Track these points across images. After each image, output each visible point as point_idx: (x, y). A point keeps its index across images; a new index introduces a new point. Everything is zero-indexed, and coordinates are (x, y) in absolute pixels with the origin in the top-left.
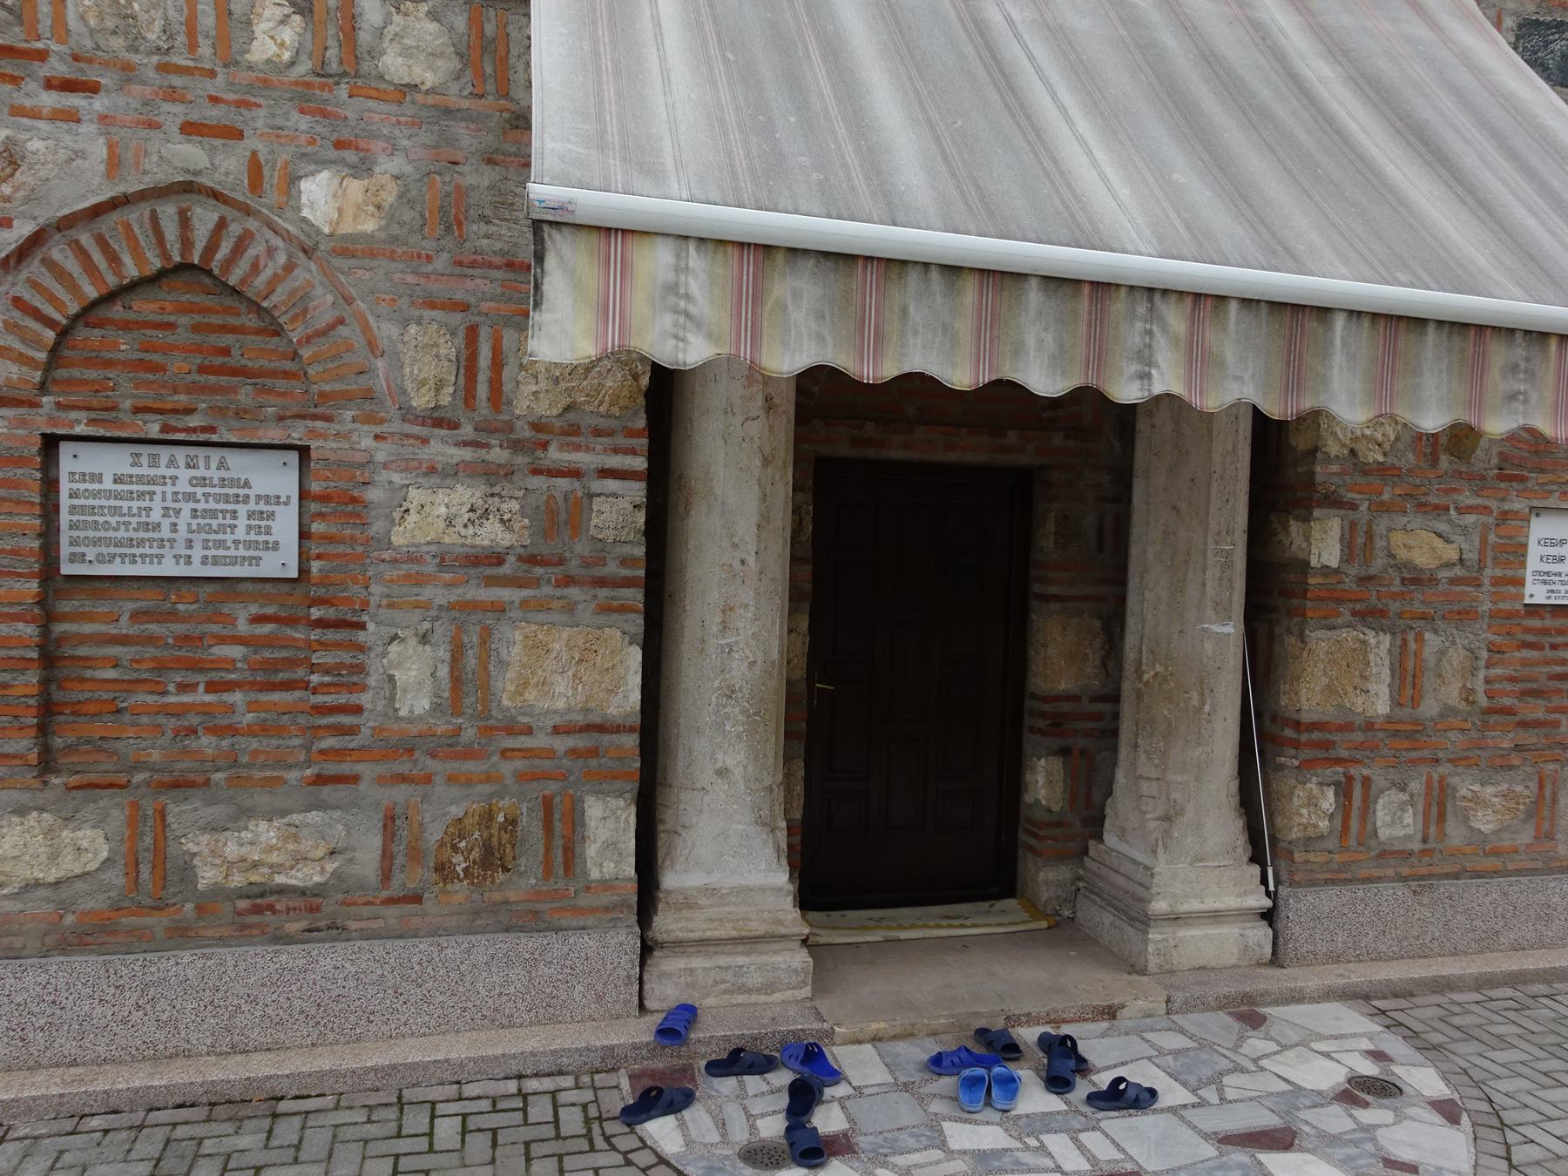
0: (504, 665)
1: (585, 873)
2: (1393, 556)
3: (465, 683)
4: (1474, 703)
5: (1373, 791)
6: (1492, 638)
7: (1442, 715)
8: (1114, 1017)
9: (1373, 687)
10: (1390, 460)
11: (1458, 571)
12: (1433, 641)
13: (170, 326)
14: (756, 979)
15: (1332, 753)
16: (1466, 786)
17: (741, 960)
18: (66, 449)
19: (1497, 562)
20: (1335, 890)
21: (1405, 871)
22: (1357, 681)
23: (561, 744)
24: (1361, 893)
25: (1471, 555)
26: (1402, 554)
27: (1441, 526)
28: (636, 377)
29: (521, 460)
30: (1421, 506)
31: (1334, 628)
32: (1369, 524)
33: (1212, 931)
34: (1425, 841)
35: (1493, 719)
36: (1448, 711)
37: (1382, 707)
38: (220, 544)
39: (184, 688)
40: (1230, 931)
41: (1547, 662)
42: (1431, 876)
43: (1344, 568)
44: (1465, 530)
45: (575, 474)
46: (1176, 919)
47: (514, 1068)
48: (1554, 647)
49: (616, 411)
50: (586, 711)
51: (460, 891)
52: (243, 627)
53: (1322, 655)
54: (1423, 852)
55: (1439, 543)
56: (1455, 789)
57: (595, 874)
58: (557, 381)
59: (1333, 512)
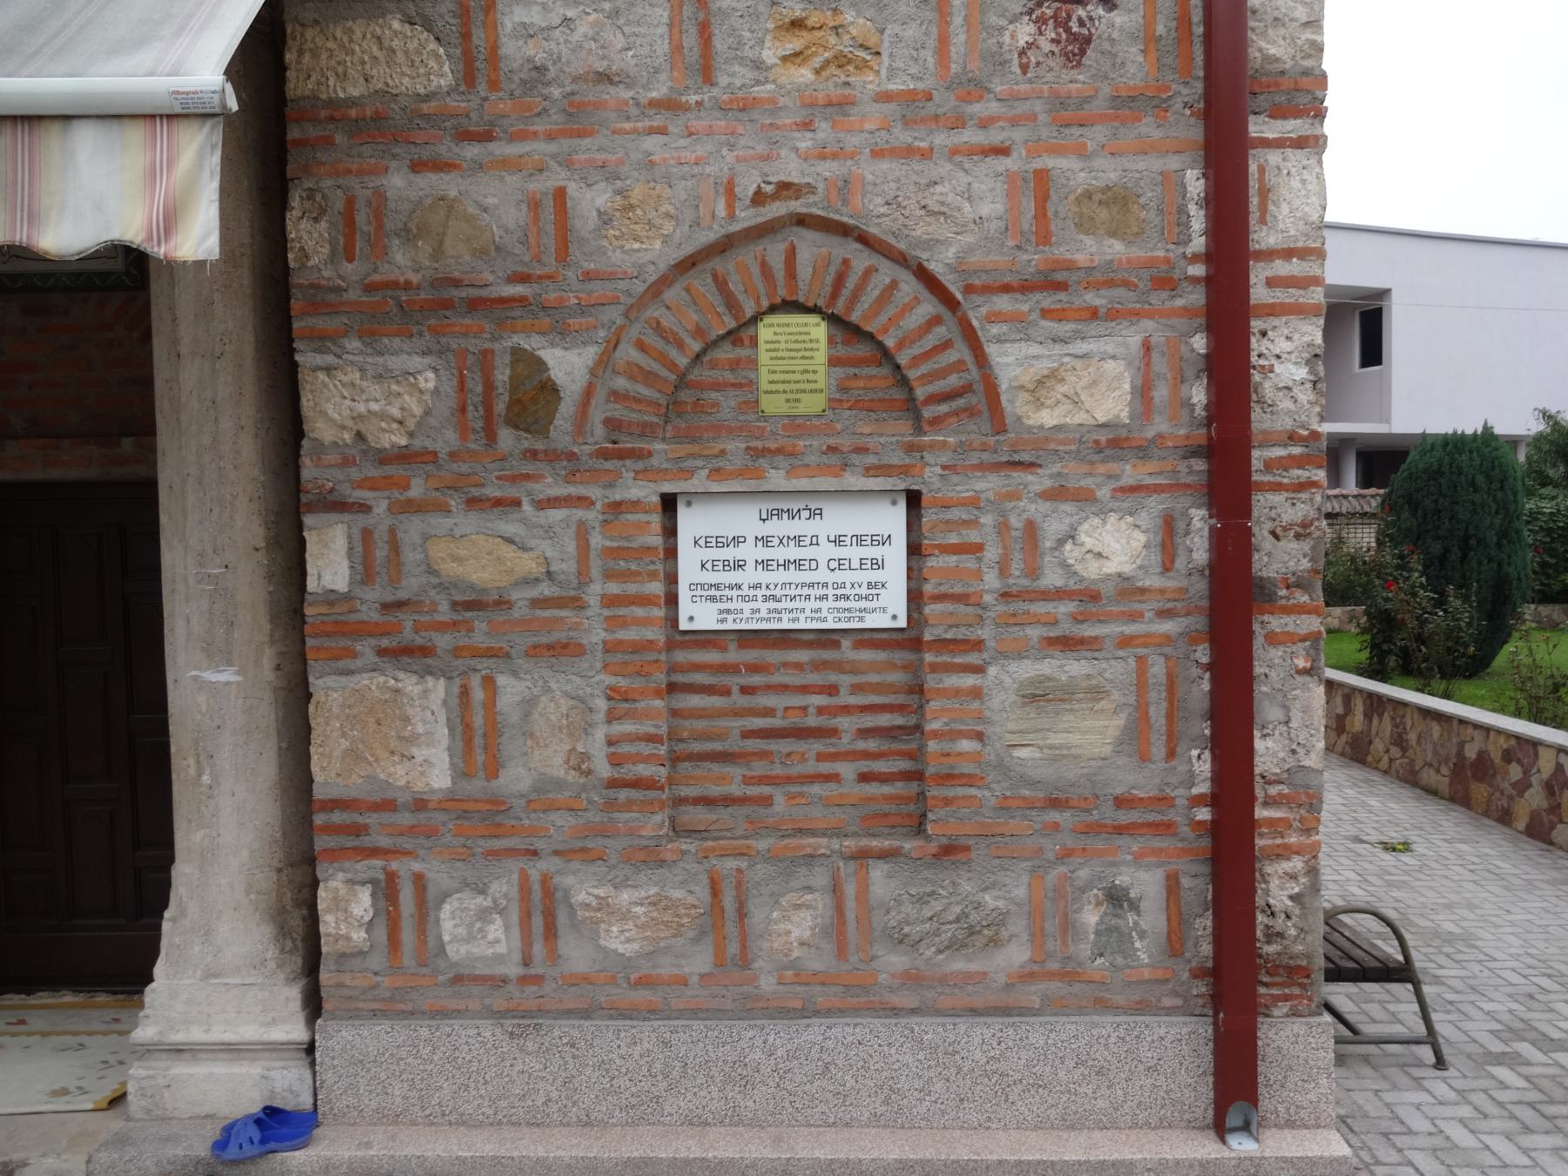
2: (436, 573)
4: (589, 772)
5: (431, 892)
6: (609, 680)
7: (536, 789)
9: (419, 753)
10: (418, 443)
11: (546, 590)
12: (511, 690)
15: (366, 841)
16: (583, 888)
19: (609, 575)
20: (385, 1025)
21: (499, 1003)
24: (424, 1032)
25: (564, 566)
26: (450, 569)
27: (511, 528)
30: (473, 503)
31: (350, 673)
32: (392, 531)
34: (527, 961)
35: (623, 795)
36: (545, 785)
37: (439, 778)
40: (249, 1070)
41: (738, 713)
42: (542, 1012)
43: (357, 591)
44: (549, 532)
46: (178, 1051)
48: (745, 690)
53: (335, 710)
54: (523, 980)
55: (509, 552)
56: (567, 893)
59: (333, 517)
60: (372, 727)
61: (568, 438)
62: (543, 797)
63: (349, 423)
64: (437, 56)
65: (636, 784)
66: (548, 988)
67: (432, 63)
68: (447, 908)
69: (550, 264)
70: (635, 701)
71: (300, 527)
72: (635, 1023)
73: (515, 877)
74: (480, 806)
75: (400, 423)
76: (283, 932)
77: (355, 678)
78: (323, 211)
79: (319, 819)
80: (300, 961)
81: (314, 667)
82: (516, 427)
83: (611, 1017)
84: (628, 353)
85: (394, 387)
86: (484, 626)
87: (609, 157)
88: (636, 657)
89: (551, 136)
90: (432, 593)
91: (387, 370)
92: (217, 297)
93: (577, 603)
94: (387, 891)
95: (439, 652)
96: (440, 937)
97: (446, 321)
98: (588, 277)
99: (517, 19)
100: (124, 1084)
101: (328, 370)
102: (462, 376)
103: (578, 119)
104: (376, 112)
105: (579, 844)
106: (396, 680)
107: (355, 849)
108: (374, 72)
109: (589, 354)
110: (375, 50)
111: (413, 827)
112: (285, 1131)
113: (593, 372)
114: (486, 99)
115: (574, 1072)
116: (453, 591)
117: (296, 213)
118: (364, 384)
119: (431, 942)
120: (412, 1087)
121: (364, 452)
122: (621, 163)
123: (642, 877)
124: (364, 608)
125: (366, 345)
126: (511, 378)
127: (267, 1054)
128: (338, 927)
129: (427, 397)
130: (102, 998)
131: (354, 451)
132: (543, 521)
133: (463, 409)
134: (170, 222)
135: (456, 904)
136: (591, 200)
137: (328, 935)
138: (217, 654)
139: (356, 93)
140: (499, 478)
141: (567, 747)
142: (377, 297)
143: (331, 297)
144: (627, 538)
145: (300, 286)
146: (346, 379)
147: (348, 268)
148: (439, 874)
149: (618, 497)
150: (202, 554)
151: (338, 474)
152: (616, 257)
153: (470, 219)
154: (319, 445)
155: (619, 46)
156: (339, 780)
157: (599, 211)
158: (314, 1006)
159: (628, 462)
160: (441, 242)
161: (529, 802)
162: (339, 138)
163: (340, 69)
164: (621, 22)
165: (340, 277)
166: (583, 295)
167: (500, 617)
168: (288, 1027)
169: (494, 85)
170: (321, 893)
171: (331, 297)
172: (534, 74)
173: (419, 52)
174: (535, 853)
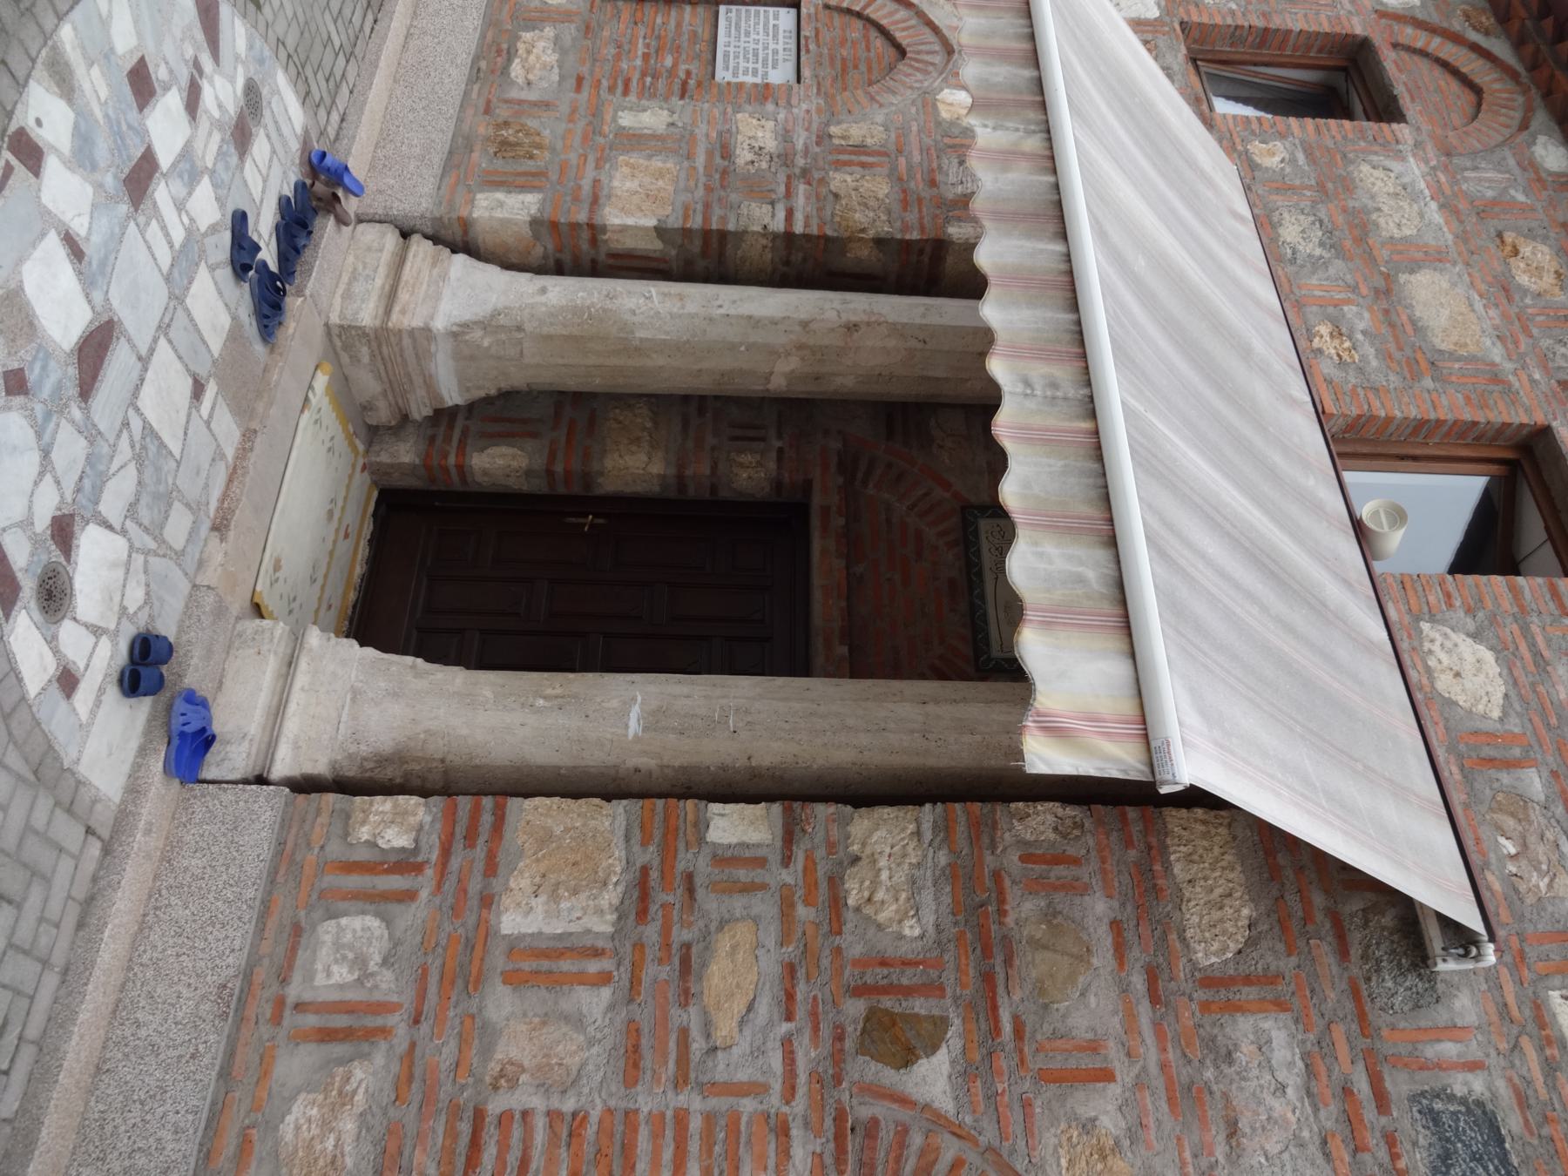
0: (650, 157)
1: (481, 191)
2: (720, 928)
3: (634, 141)
4: (496, 1088)
5: (394, 908)
6: (595, 1116)
8: (215, 528)
9: (539, 903)
10: (849, 916)
11: (698, 1045)
12: (594, 1002)
13: (868, 49)
14: (358, 288)
15: (458, 845)
16: (367, 1077)
17: (379, 282)
18: (793, 11)
19: (710, 1118)
20: (266, 851)
21: (261, 974)
22: (553, 877)
23: (586, 184)
24: (250, 893)
25: (721, 1067)
26: (724, 943)
27: (764, 1009)
28: (863, 230)
29: (797, 171)
30: (790, 970)
31: (627, 838)
32: (763, 887)
33: (263, 699)
34: (300, 1007)
35: (465, 1128)
37: (511, 922)
38: (736, 57)
39: (648, 46)
40: (255, 725)
42: (240, 1020)
43: (706, 850)
44: (758, 1052)
45: (788, 194)
47: (349, 118)
49: (837, 219)
50: (609, 197)
51: (491, 131)
52: (683, 67)
54: (280, 1003)
55: (739, 1006)
57: (479, 196)
58: (856, 189)
59: (779, 831)
60: (571, 857)
61: (856, 1076)
62: (477, 1033)
63: (868, 851)
64: (1224, 949)
65: (475, 1144)
66: (265, 1030)
67: (1216, 946)
68: (373, 923)
69: (1036, 1063)
70: (569, 1145)
71: (769, 798)
72: (200, 1133)
73: (395, 999)
74: (476, 963)
75: (869, 900)
76: (382, 760)
77: (622, 844)
78: (1065, 836)
79: (488, 802)
80: (351, 774)
81: (634, 805)
82: (867, 1019)
83: (214, 1103)
84: (950, 1148)
85: (904, 895)
86: (664, 976)
87: (1152, 1133)
88: (617, 1147)
89: (1164, 1066)
90: (701, 924)
91: (920, 889)
92: (978, 738)
93: (681, 1081)
94: (405, 863)
95: (640, 928)
96: (345, 914)
97: (970, 950)
98: (1026, 1105)
99: (1274, 1034)
100: (271, 617)
101: (918, 834)
102: (917, 964)
103: (1187, 1098)
104: (1162, 890)
105: (418, 1072)
106: (616, 884)
107: (452, 834)
108: (1198, 889)
109: (946, 1104)
110: (1218, 891)
111: (465, 891)
112: (187, 753)
113: (927, 1107)
114: (1191, 1000)
115: (162, 1057)
116: (701, 945)
117: (1060, 812)
118: (906, 867)
119: (342, 905)
120: (195, 877)
121: (841, 863)
122: (1149, 1147)
123: (367, 1147)
124: (690, 856)
125: (943, 870)
126: (917, 1015)
127: (266, 739)
128: (377, 813)
129: (895, 927)
130: (352, 596)
131: (841, 854)
132: (770, 1045)
133: (884, 963)
134: (1055, 731)
135: (377, 933)
136: (1105, 1109)
137: (371, 804)
138: (654, 720)
139: (1176, 871)
140: (815, 998)
141: (526, 1063)
142: (988, 883)
143: (986, 840)
144: (749, 1142)
145: (994, 812)
146: (910, 849)
147: (1015, 857)
148: (412, 917)
149: (794, 1132)
150: (747, 712)
151: (820, 836)
152: (1049, 1139)
153: (1072, 978)
154: (848, 821)
155: (1268, 1147)
156: (523, 823)
157: (1094, 1120)
158: (304, 786)
159: (832, 1145)
160: (1045, 947)
161: (473, 1017)
162: (1133, 854)
163: (1196, 857)
164: (1294, 1151)
165: (1005, 849)
166: (1006, 1098)
167: (672, 993)
168: (288, 760)
169: (1205, 1007)
170: (414, 800)
171: (986, 840)
172: (1223, 1051)
173: (1224, 932)
174: (417, 1021)
